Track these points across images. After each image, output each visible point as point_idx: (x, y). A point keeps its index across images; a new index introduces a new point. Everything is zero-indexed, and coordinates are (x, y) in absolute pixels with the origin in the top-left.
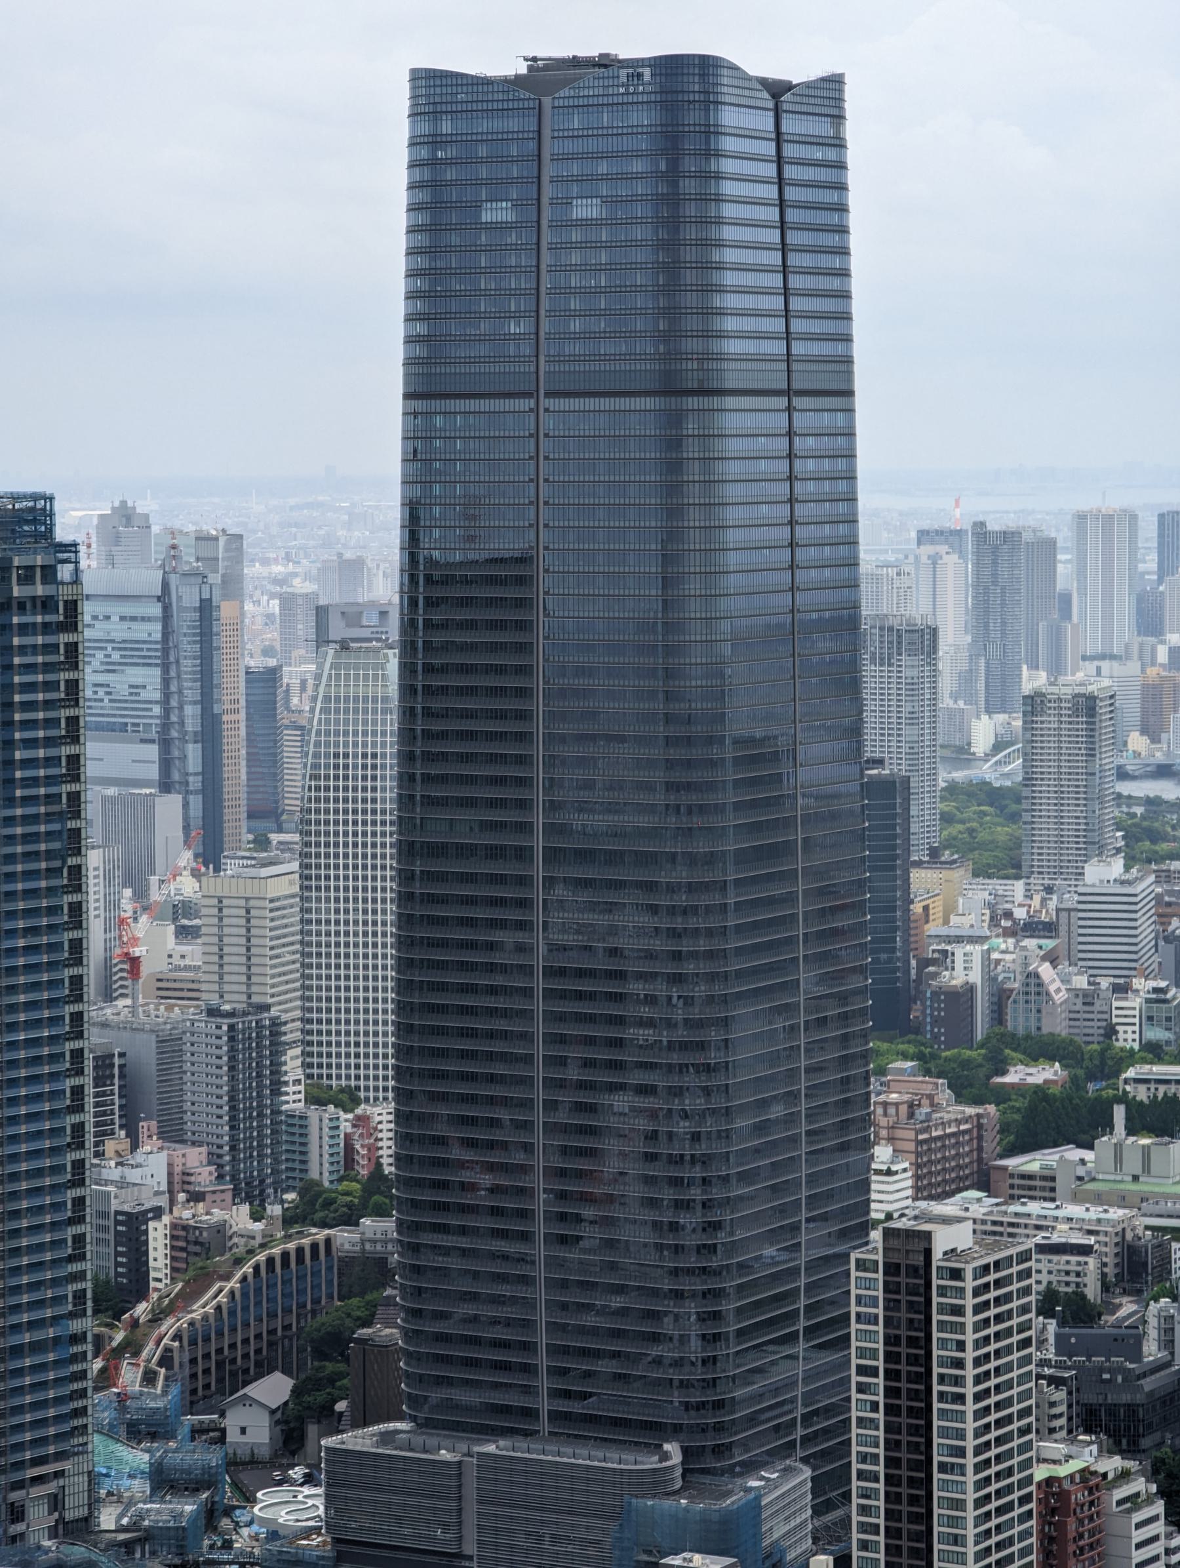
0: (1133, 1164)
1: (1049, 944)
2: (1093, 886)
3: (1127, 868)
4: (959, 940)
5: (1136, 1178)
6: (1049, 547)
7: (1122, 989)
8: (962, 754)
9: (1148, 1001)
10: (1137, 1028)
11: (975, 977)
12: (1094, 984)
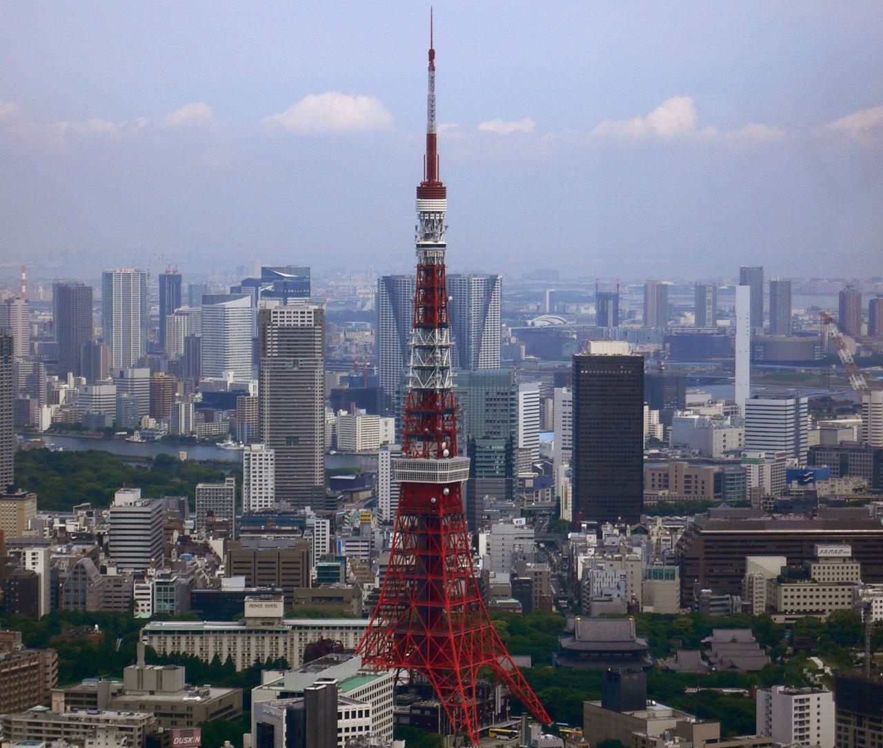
0: (150, 683)
1: (89, 548)
2: (120, 506)
3: (142, 497)
4: (29, 545)
5: (152, 693)
6: (90, 289)
7: (140, 577)
8: (30, 429)
9: (158, 583)
10: (150, 602)
11: (40, 569)
12: (121, 573)
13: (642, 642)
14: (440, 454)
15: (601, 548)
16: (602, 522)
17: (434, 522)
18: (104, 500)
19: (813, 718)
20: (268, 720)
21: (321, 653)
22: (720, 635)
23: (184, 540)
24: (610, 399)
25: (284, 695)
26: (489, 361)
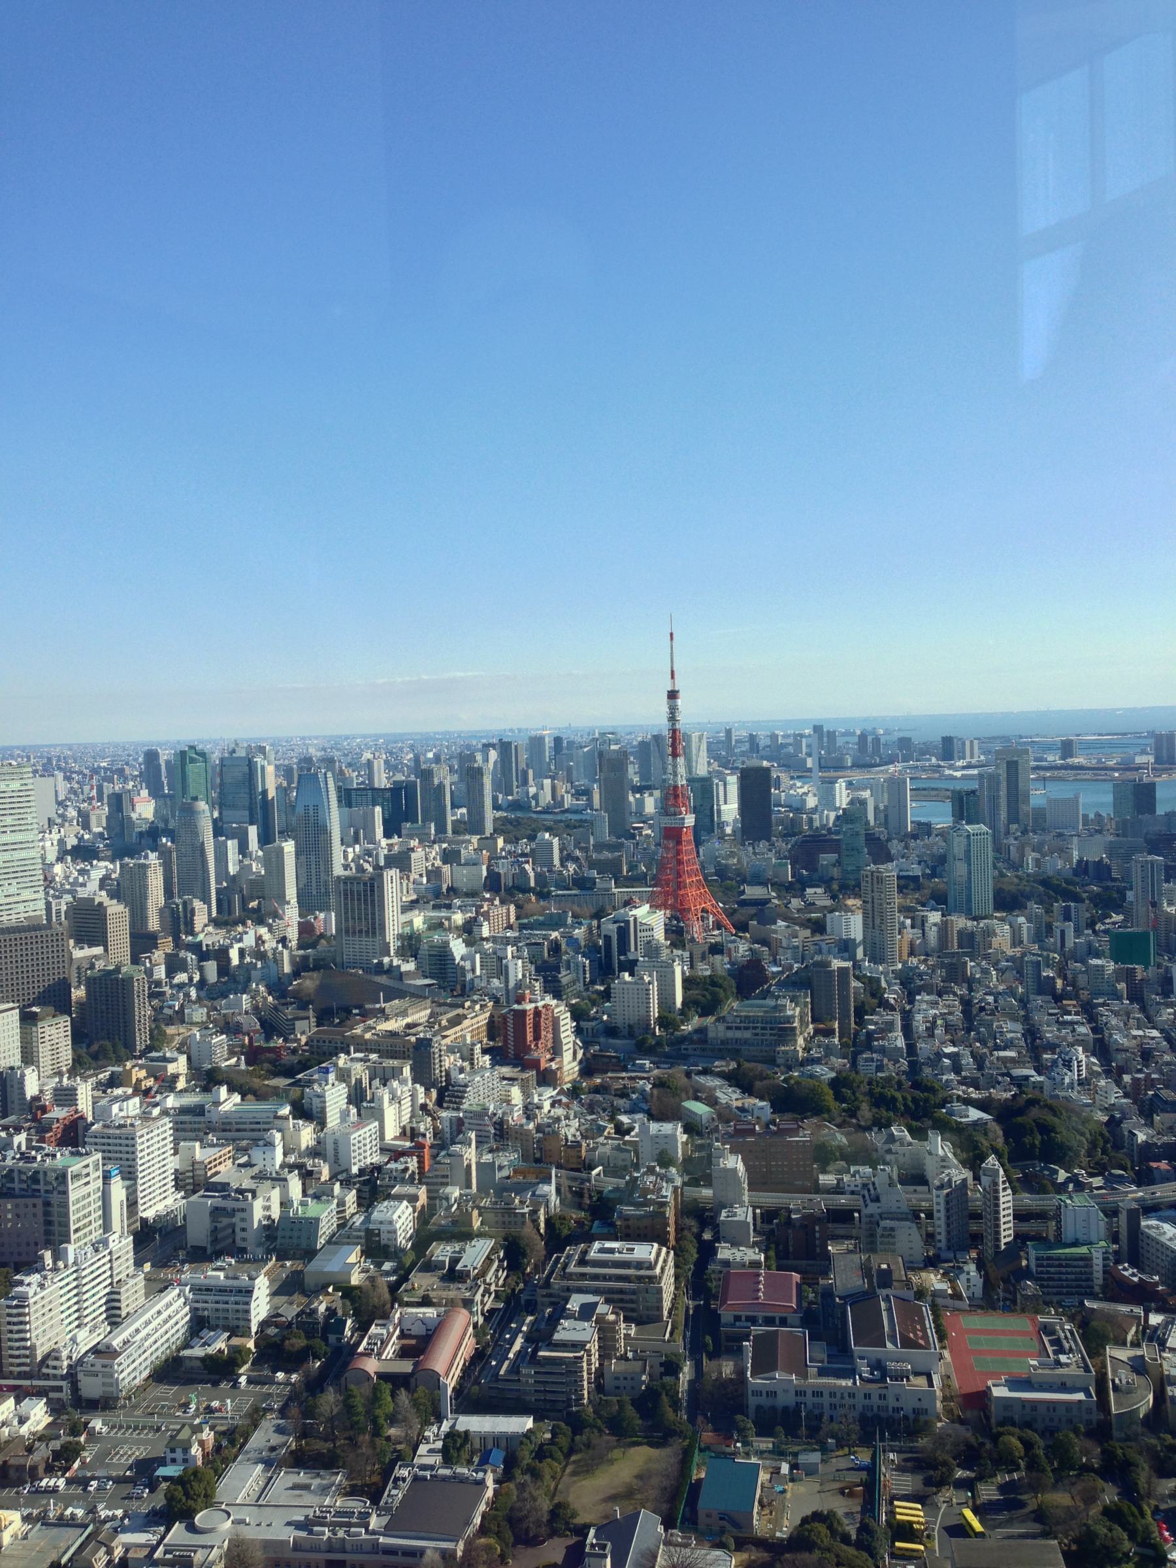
13: (774, 894)
14: (681, 813)
15: (755, 854)
16: (754, 840)
17: (679, 842)
18: (532, 838)
19: (852, 926)
20: (609, 934)
21: (628, 903)
22: (809, 891)
23: (569, 855)
24: (756, 787)
25: (615, 922)
26: (702, 770)
